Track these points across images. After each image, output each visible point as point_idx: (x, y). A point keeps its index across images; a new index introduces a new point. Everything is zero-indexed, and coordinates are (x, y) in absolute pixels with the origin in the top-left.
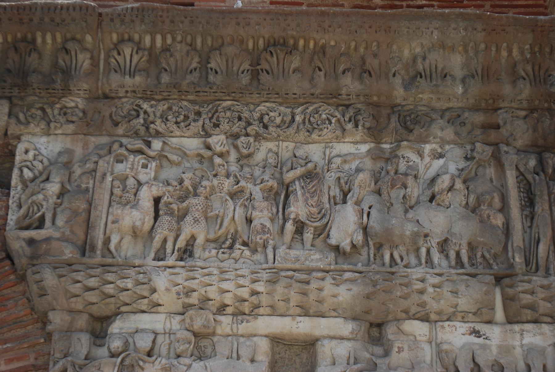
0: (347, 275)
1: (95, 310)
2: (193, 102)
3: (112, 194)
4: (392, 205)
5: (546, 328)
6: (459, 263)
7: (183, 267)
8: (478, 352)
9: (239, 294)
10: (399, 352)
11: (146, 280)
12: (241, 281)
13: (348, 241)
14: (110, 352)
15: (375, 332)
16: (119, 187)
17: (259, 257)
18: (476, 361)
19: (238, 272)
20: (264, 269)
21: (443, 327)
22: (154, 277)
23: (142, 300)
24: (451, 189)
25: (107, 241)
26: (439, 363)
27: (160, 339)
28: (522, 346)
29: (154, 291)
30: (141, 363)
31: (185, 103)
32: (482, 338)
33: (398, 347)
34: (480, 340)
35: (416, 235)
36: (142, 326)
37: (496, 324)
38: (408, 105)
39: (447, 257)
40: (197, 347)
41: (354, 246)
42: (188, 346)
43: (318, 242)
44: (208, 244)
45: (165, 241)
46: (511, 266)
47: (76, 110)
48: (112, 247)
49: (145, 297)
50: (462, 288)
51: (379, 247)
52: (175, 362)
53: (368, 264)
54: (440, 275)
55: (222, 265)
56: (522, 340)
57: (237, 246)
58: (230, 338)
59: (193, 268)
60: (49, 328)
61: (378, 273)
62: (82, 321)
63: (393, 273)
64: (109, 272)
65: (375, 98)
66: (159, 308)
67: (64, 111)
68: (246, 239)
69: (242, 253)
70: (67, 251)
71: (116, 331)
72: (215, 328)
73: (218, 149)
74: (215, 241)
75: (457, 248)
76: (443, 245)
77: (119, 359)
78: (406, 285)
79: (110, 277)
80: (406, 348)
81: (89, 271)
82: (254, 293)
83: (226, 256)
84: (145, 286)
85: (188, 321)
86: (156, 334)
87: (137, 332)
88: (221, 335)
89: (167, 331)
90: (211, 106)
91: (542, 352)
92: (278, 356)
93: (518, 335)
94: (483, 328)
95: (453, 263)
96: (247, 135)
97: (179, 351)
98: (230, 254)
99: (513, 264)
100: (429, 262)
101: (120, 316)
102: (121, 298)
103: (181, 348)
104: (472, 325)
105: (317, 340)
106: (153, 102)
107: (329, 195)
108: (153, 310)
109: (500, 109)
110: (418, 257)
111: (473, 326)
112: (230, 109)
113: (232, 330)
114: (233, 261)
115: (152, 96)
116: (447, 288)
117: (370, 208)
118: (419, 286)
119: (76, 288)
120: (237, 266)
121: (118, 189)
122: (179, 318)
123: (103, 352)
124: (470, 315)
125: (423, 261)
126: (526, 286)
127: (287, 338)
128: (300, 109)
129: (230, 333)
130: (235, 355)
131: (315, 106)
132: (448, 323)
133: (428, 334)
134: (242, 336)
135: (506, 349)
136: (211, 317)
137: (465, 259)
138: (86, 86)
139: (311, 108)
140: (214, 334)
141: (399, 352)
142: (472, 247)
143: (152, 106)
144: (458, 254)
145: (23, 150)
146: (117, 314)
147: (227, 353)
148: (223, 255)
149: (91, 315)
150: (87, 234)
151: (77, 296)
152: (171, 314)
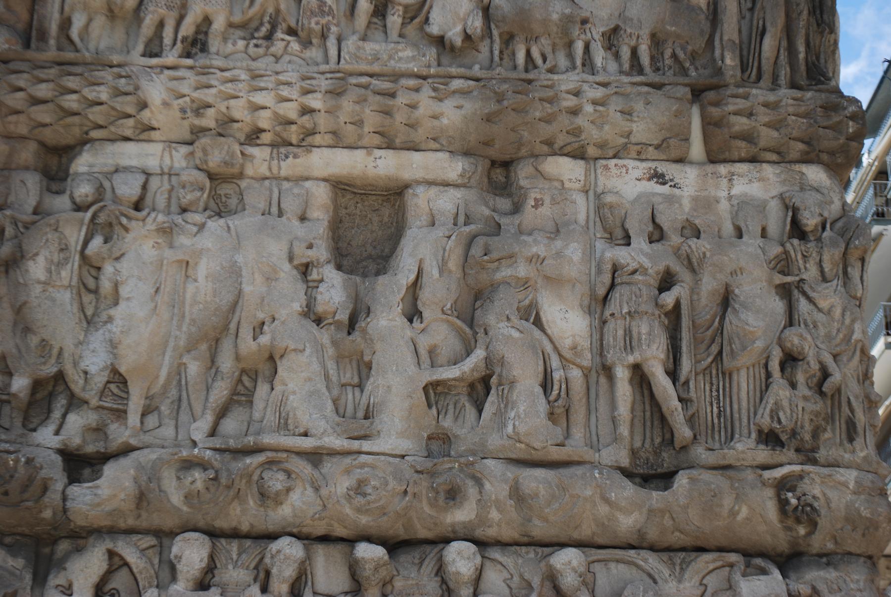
0: (457, 84)
1: (48, 135)
5: (769, 171)
6: (636, 66)
7: (191, 68)
8: (660, 208)
9: (281, 112)
10: (536, 207)
11: (130, 88)
12: (285, 92)
13: (459, 28)
14: (74, 203)
15: (499, 175)
17: (314, 53)
18: (657, 220)
19: (281, 77)
20: (323, 73)
21: (606, 168)
22: (144, 83)
23: (125, 121)
25: (66, 24)
26: (599, 224)
27: (154, 183)
28: (730, 198)
29: (143, 105)
30: (124, 221)
32: (667, 186)
33: (535, 199)
34: (665, 189)
35: (567, 20)
36: (125, 162)
37: (691, 163)
39: (617, 56)
40: (214, 196)
41: (467, 37)
42: (199, 194)
43: (411, 30)
44: (232, 30)
45: (161, 25)
46: (719, 72)
48: (74, 33)
49: (129, 116)
50: (639, 106)
51: (508, 39)
52: (179, 220)
53: (490, 67)
54: (605, 85)
55: (254, 65)
56: (730, 189)
57: (279, 35)
58: (267, 182)
59: (206, 70)
61: (505, 80)
62: (27, 153)
63: (530, 82)
64: (70, 74)
66: (153, 133)
68: (293, 24)
71: (82, 169)
72: (242, 166)
74: (243, 26)
75: (633, 43)
76: (612, 38)
77: (89, 214)
78: (550, 101)
79: (71, 82)
80: (547, 200)
81: (37, 72)
82: (306, 111)
83: (261, 51)
84: (129, 98)
85: (199, 154)
86: (148, 174)
87: (116, 171)
88: (252, 178)
91: (761, 207)
92: (344, 211)
93: (725, 181)
94: (670, 170)
95: (626, 66)
97: (184, 202)
98: (268, 48)
99: (721, 68)
100: (588, 63)
101: (88, 146)
102: (91, 117)
103: (188, 197)
104: (652, 165)
105: (407, 186)
108: (142, 137)
110: (571, 56)
111: (654, 167)
113: (270, 169)
114: (272, 59)
116: (616, 104)
118: (570, 102)
119: (16, 100)
120: (278, 67)
122: (184, 150)
123: (62, 202)
124: (651, 148)
125: (579, 62)
126: (741, 104)
127: (358, 183)
129: (268, 174)
130: (274, 210)
132: (613, 162)
133: (583, 178)
134: (287, 179)
135: (705, 203)
136: (237, 148)
137: (645, 60)
140: (241, 175)
141: (536, 207)
142: (656, 41)
144: (634, 52)
146: (84, 143)
147: (262, 205)
148: (256, 49)
149: (42, 144)
150: (32, 11)
151: (17, 112)
152: (171, 143)
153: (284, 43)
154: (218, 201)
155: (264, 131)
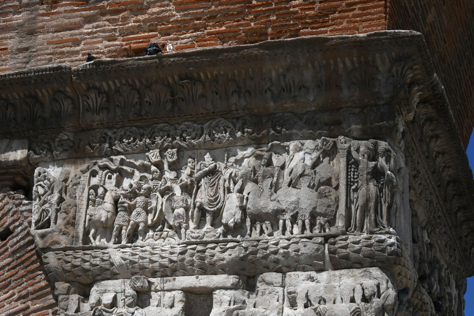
0: (230, 245)
2: (138, 127)
3: (89, 199)
4: (263, 190)
6: (303, 229)
7: (130, 247)
10: (262, 295)
13: (232, 220)
16: (93, 194)
23: (107, 272)
24: (302, 175)
29: (112, 264)
31: (134, 128)
33: (262, 292)
38: (279, 113)
47: (68, 141)
57: (166, 229)
58: (159, 293)
59: (136, 248)
60: (56, 293)
65: (256, 111)
67: (61, 143)
69: (168, 234)
70: (62, 242)
73: (154, 160)
82: (171, 261)
84: (107, 262)
89: (123, 291)
90: (150, 129)
96: (173, 148)
98: (161, 235)
106: (115, 130)
107: (224, 186)
108: (114, 277)
109: (342, 108)
112: (162, 130)
114: (163, 240)
115: (114, 126)
117: (248, 194)
121: (93, 196)
128: (207, 124)
131: (217, 120)
133: (281, 281)
138: (71, 124)
139: (214, 123)
142: (313, 216)
143: (114, 133)
145: (38, 174)
153: (167, 232)
154: (142, 302)
155: (158, 271)
